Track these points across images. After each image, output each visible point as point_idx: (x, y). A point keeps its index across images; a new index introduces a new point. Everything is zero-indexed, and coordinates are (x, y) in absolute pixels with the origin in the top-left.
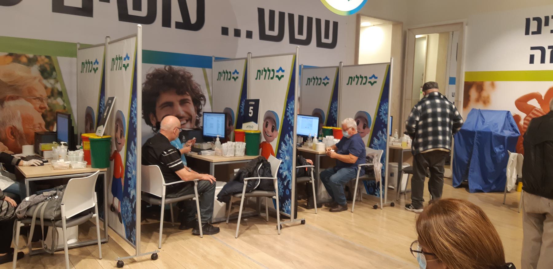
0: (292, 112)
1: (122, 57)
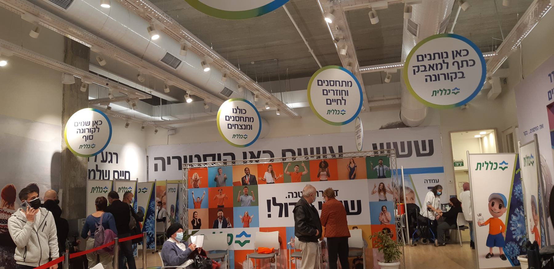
0: (519, 192)
1: (529, 157)
